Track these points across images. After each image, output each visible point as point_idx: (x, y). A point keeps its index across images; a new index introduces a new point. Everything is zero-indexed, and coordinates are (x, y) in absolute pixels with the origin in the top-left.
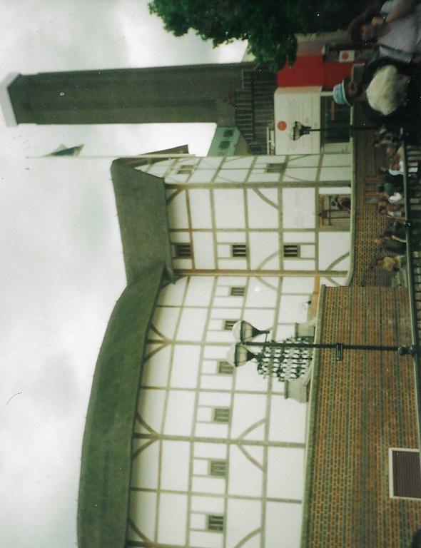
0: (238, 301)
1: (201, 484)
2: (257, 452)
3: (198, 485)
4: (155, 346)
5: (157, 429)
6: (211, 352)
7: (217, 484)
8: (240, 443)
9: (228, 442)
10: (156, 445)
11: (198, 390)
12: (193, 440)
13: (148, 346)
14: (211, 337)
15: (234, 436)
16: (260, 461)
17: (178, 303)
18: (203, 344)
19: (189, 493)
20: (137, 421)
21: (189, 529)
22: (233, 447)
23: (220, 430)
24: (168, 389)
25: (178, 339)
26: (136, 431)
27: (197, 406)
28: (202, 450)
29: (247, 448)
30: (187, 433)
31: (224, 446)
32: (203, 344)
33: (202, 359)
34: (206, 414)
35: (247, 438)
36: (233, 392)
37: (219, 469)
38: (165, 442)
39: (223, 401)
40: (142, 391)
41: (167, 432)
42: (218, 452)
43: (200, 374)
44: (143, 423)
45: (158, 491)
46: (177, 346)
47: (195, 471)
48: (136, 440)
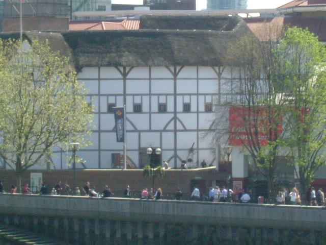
0: (202, 108)
1: (104, 100)
4: (172, 69)
5: (127, 77)
6: (120, 100)
12: (125, 95)
14: (179, 98)
17: (199, 77)
18: (175, 95)
23: (130, 108)
24: (150, 79)
27: (142, 95)
30: (128, 92)
33: (166, 95)
34: (138, 100)
39: (145, 108)
41: (128, 81)
43: (159, 95)
44: (132, 68)
45: (99, 79)
46: (172, 81)
47: (110, 97)
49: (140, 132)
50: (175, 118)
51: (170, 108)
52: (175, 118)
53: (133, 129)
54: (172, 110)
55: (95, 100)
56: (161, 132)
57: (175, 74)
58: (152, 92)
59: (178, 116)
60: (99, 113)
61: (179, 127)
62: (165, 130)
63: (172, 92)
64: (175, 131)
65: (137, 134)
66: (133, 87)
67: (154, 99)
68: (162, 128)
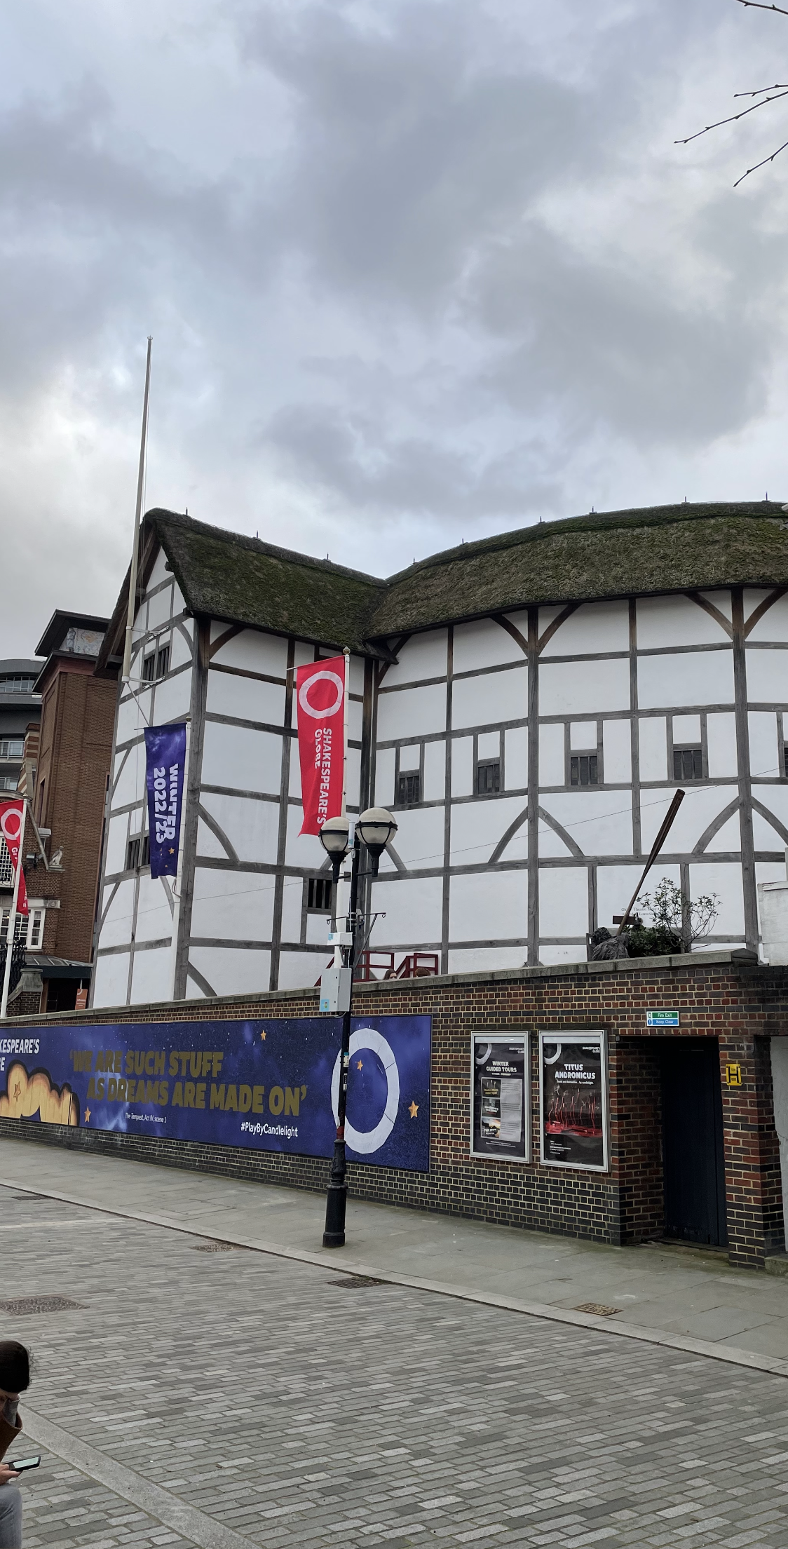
2: (517, 849)
3: (462, 747)
7: (464, 783)
8: (533, 814)
9: (533, 790)
10: (521, 655)
11: (634, 714)
12: (533, 721)
13: (729, 594)
15: (544, 800)
16: (500, 860)
19: (448, 735)
20: (559, 610)
21: (396, 744)
22: (522, 802)
23: (553, 770)
25: (749, 653)
26: (540, 611)
27: (599, 717)
28: (518, 739)
29: (525, 827)
30: (542, 712)
31: (525, 785)
32: (742, 707)
33: (703, 711)
34: (584, 738)
35: (542, 824)
36: (636, 786)
37: (488, 780)
38: (525, 669)
39: (615, 768)
40: (626, 603)
42: (515, 776)
43: (671, 713)
48: (525, 613)
49: (593, 864)
50: (745, 805)
51: (722, 761)
52: (745, 805)
53: (567, 853)
54: (733, 772)
55: (436, 750)
56: (683, 861)
57: (740, 630)
58: (641, 706)
59: (757, 791)
60: (448, 802)
61: (765, 838)
62: (700, 855)
63: (730, 699)
64: (749, 857)
65: (583, 871)
66: (563, 688)
67: (653, 730)
68: (688, 849)
